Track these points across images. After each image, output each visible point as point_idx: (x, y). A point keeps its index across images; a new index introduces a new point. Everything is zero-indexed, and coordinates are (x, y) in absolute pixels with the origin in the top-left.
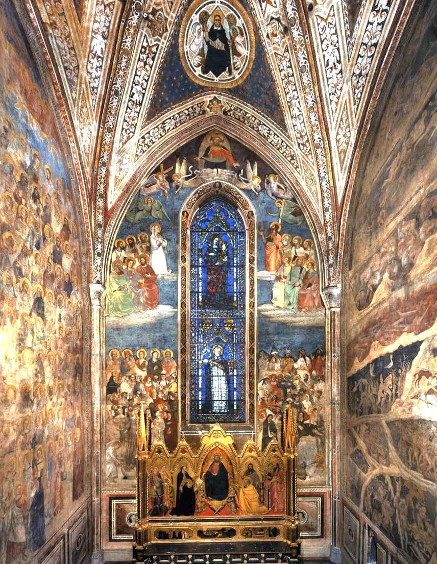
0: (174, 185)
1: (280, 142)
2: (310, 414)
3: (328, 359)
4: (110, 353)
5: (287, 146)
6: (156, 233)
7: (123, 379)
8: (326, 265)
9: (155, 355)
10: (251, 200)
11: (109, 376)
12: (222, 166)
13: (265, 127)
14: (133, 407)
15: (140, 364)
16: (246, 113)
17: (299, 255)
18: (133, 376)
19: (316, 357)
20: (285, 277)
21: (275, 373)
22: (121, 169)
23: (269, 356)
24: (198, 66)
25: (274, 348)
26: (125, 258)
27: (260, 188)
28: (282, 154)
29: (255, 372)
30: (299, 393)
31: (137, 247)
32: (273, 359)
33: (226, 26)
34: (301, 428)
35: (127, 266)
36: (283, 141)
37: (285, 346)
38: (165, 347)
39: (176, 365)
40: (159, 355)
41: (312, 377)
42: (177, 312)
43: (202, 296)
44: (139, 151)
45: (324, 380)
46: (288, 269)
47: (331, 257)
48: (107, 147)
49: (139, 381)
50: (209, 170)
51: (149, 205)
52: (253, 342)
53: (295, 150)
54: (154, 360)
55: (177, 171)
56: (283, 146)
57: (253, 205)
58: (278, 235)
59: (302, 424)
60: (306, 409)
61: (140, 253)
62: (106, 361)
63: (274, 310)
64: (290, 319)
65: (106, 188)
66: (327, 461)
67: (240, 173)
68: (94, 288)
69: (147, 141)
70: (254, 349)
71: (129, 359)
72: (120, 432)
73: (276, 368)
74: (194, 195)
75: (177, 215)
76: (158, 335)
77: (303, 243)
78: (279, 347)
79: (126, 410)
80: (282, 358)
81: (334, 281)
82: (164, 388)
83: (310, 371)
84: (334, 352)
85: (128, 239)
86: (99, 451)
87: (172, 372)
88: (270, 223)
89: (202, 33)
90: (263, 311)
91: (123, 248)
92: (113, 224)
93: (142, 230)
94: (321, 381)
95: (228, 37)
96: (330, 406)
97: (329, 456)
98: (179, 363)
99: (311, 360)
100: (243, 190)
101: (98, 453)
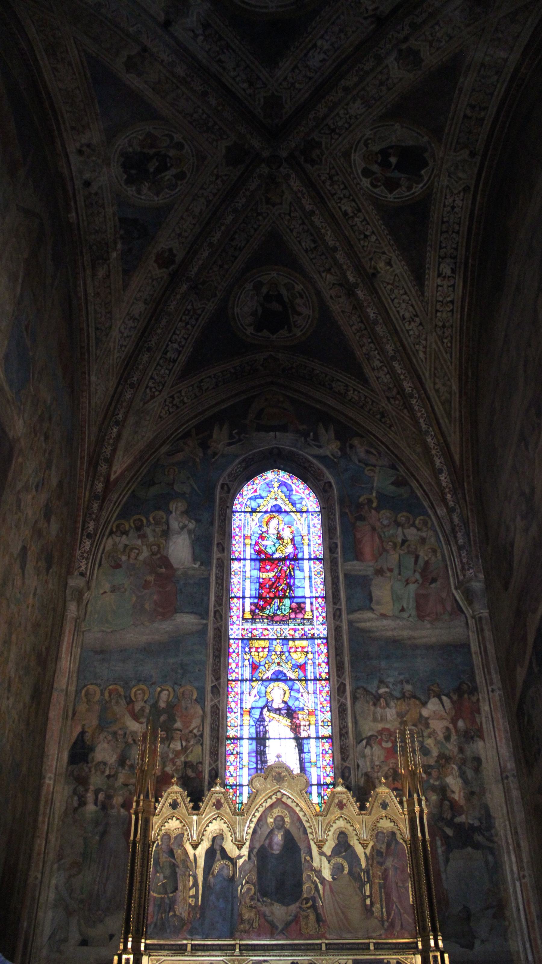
0: (209, 452)
1: (363, 399)
2: (462, 802)
3: (484, 699)
4: (83, 692)
5: (373, 402)
6: (178, 512)
7: (102, 737)
8: (454, 549)
9: (164, 695)
10: (328, 467)
11: (79, 729)
12: (284, 429)
13: (340, 383)
14: (115, 790)
15: (136, 711)
16: (313, 369)
17: (409, 538)
18: (120, 732)
19: (461, 696)
20: (391, 570)
21: (388, 726)
22: (136, 432)
23: (375, 697)
24: (250, 325)
25: (381, 682)
26: (126, 546)
27: (339, 453)
28: (369, 412)
29: (350, 725)
30: (437, 762)
31: (148, 531)
32: (382, 702)
33: (284, 291)
34: (449, 832)
35: (129, 557)
36: (366, 397)
37: (402, 677)
38: (183, 683)
39: (201, 712)
40: (172, 695)
41: (457, 731)
42: (206, 625)
43: (251, 604)
44: (164, 412)
45: (482, 737)
46: (394, 557)
47: (459, 535)
48: (125, 404)
49: (130, 741)
50: (262, 434)
51: (172, 477)
52: (343, 673)
53: (384, 405)
54: (162, 705)
55: (215, 436)
56: (368, 403)
57: (331, 473)
58: (373, 511)
59: (450, 823)
60: (453, 792)
61: (151, 539)
62: (75, 705)
63: (377, 619)
64: (406, 633)
65: (114, 451)
66: (514, 904)
67: (309, 436)
68: (76, 582)
69: (176, 401)
70: (345, 685)
71: (117, 702)
72: (85, 839)
73: (389, 716)
74: (239, 463)
75: (214, 488)
76: (172, 661)
77: (414, 521)
78: (391, 680)
79: (101, 796)
80: (398, 699)
81: (471, 571)
82: (177, 754)
83: (454, 722)
84: (492, 684)
85: (135, 521)
86: (39, 876)
87: (193, 725)
88: (359, 497)
89: (256, 298)
90: (357, 622)
91: (126, 533)
92: (115, 499)
93: (158, 508)
94: (476, 738)
95: (286, 300)
96: (500, 786)
97: (515, 892)
98: (208, 709)
99: (452, 702)
100: (316, 457)
101: (36, 878)
